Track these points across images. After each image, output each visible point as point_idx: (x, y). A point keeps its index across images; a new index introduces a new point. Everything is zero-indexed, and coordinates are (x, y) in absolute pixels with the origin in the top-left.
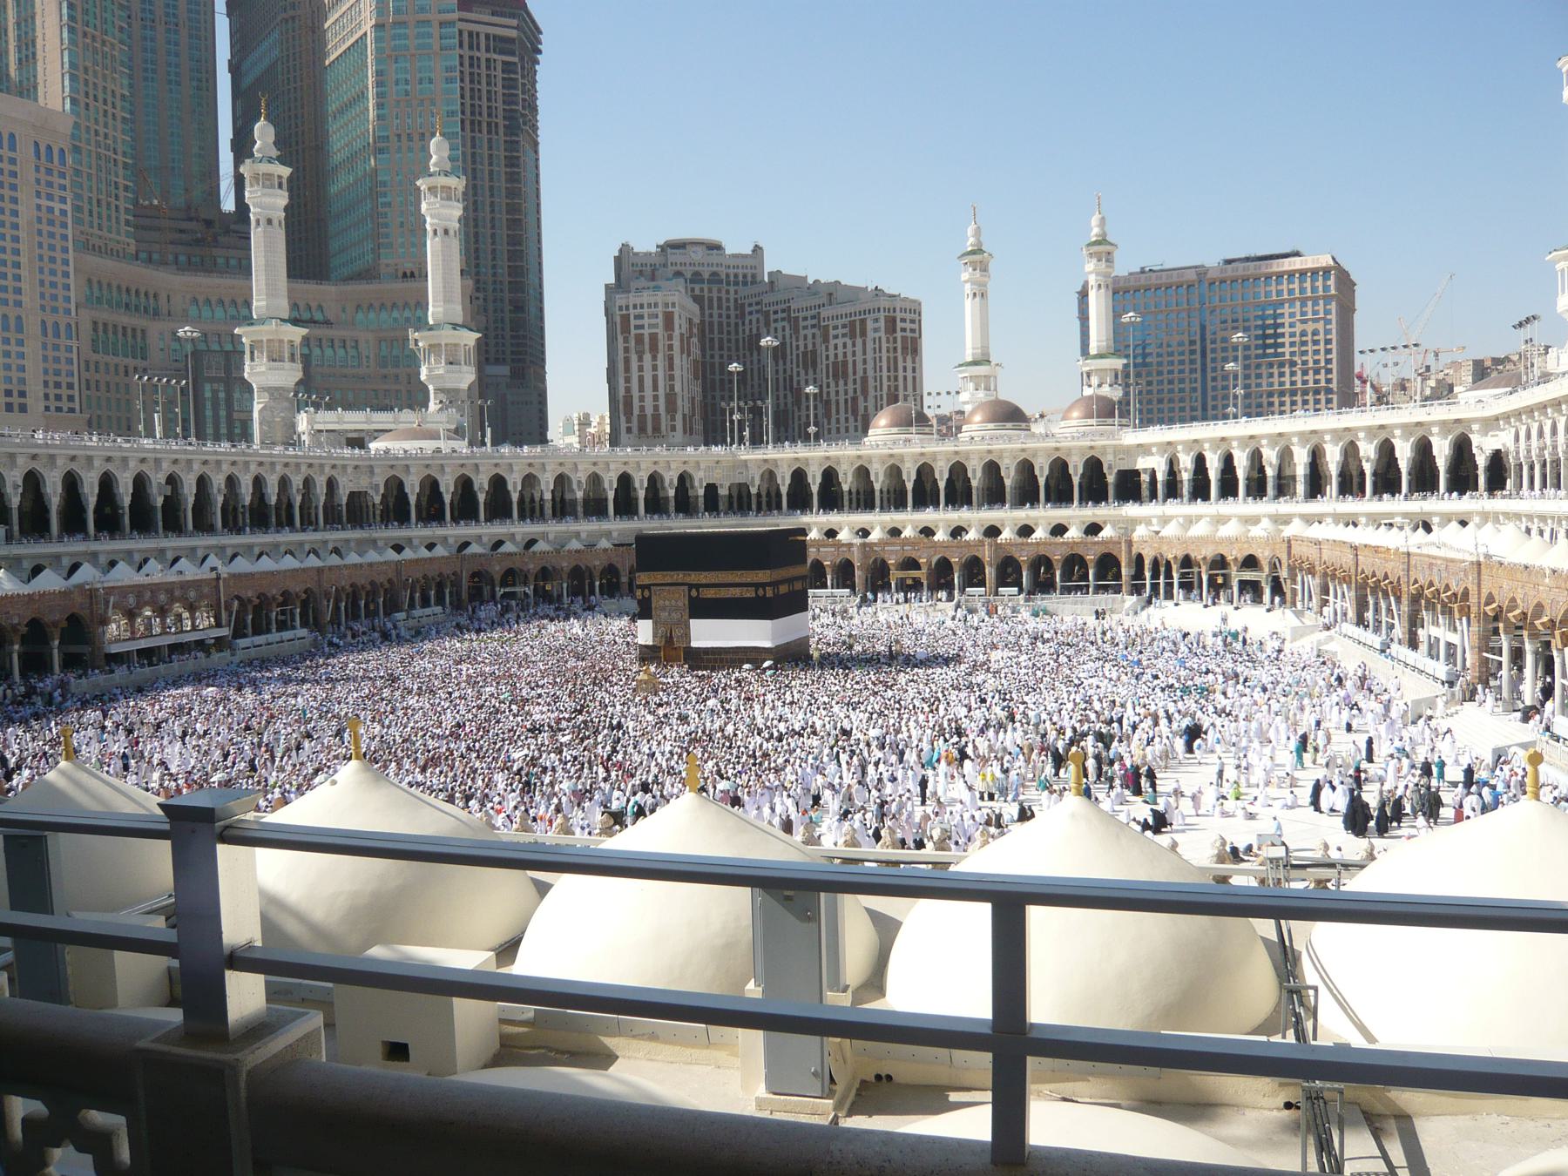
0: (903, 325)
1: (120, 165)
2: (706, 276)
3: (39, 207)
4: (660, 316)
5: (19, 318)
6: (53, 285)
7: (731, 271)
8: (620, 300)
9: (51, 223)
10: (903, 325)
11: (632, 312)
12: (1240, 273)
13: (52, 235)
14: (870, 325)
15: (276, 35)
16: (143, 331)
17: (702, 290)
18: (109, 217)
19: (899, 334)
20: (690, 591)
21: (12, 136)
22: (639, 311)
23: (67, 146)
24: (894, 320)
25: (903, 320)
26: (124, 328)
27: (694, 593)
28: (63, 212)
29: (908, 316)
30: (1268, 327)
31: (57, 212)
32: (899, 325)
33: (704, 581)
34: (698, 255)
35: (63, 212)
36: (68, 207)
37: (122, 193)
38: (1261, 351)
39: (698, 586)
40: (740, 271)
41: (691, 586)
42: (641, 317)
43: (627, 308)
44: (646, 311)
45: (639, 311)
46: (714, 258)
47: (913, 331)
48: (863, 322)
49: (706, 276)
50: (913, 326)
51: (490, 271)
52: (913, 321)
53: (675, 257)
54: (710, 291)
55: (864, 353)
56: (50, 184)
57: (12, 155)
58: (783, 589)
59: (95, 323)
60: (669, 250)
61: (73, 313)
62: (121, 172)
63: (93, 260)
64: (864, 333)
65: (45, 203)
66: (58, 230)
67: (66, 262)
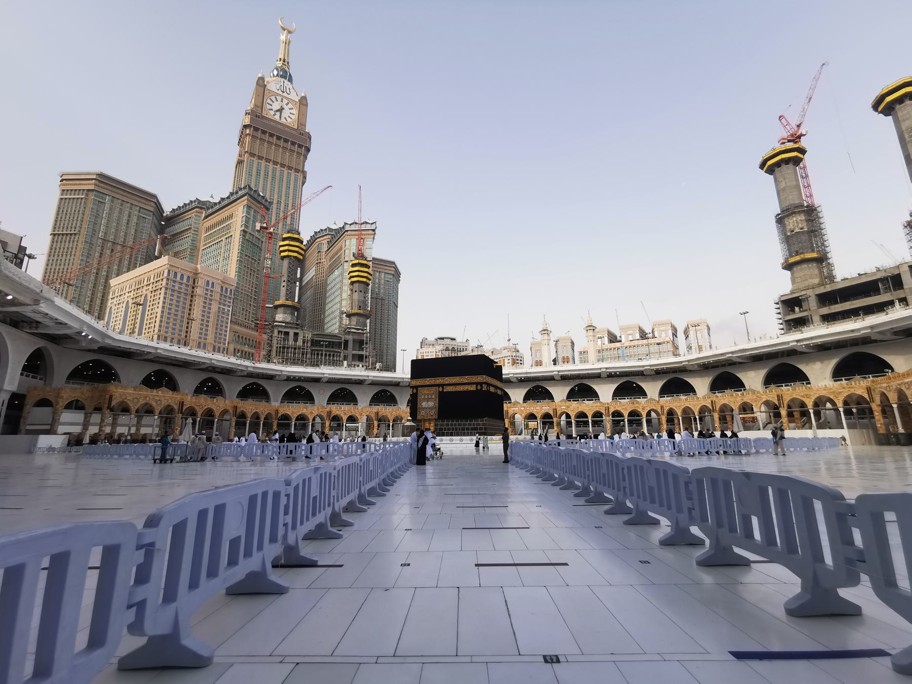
0: (517, 361)
1: (253, 298)
2: (450, 348)
3: (219, 308)
4: (434, 356)
5: (205, 344)
6: (220, 334)
7: (459, 347)
8: (421, 350)
9: (223, 313)
10: (517, 361)
11: (425, 354)
13: (223, 318)
14: (506, 361)
15: (314, 268)
16: (253, 354)
17: (449, 353)
18: (246, 314)
21: (213, 283)
22: (427, 354)
23: (233, 288)
25: (518, 360)
26: (246, 352)
27: (441, 389)
28: (229, 311)
29: (519, 359)
31: (226, 310)
34: (448, 342)
35: (229, 311)
36: (231, 309)
37: (252, 307)
39: (443, 385)
40: (462, 347)
41: (439, 385)
42: (428, 356)
43: (423, 353)
44: (430, 354)
45: (427, 354)
46: (453, 342)
48: (504, 360)
49: (450, 348)
50: (521, 362)
51: (379, 341)
52: (521, 360)
53: (440, 342)
54: (452, 353)
56: (225, 301)
57: (212, 289)
58: (492, 389)
59: (235, 349)
60: (439, 340)
61: (227, 345)
62: (252, 300)
63: (237, 328)
65: (221, 306)
66: (225, 316)
67: (227, 327)
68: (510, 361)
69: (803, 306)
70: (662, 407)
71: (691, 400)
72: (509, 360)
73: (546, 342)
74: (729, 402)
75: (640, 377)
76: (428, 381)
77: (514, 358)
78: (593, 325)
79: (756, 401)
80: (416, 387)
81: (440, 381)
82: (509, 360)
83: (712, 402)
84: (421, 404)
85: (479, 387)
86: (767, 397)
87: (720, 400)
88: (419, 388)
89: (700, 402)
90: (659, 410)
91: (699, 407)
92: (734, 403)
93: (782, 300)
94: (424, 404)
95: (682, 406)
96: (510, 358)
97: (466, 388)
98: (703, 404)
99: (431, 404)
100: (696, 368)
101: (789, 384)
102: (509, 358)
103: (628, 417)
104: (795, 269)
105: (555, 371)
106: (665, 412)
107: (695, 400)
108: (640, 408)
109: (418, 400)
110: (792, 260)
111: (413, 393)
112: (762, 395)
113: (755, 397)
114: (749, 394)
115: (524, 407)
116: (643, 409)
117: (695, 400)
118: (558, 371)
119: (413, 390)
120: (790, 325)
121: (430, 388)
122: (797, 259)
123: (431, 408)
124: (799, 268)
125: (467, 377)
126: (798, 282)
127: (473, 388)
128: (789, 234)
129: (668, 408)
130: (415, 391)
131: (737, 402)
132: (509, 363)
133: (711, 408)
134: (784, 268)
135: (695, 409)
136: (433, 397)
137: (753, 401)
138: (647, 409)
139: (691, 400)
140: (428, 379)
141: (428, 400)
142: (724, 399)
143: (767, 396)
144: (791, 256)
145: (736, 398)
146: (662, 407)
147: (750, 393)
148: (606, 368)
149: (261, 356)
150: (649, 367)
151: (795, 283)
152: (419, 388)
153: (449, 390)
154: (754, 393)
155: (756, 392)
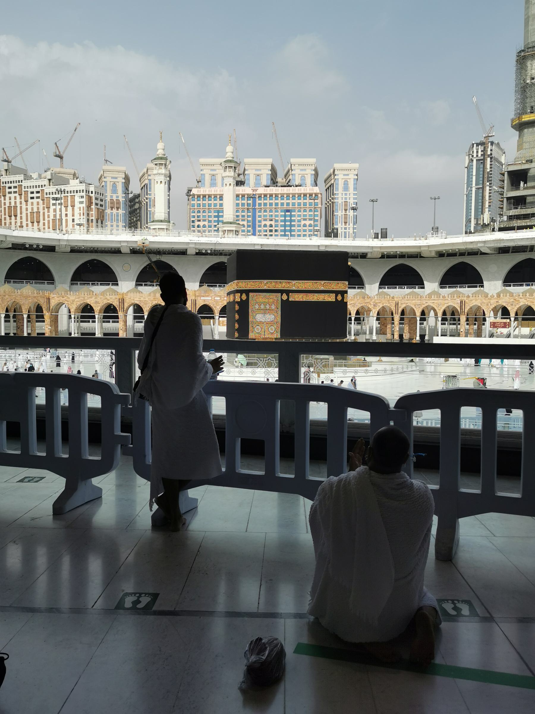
0: (97, 202)
12: (274, 192)
14: (77, 199)
19: (93, 207)
20: (282, 295)
24: (90, 198)
27: (285, 297)
30: (288, 221)
32: (94, 201)
33: (294, 288)
38: (283, 233)
39: (288, 292)
41: (281, 292)
47: (101, 206)
48: (73, 197)
50: (102, 203)
52: (102, 200)
55: (73, 215)
64: (73, 202)
68: (84, 200)
69: (528, 183)
70: (397, 304)
71: (436, 298)
72: (82, 197)
73: (162, 178)
74: (481, 304)
75: (359, 259)
76: (265, 284)
77: (91, 195)
78: (235, 160)
79: (512, 305)
80: (247, 292)
81: (283, 284)
82: (82, 197)
83: (461, 302)
84: (254, 318)
85: (339, 298)
86: (525, 301)
87: (472, 300)
88: (251, 294)
89: (446, 302)
90: (393, 308)
91: (443, 308)
92: (488, 305)
93: (509, 170)
94: (259, 317)
95: (423, 304)
96: (84, 194)
97: (321, 298)
98: (450, 304)
99: (270, 317)
100: (433, 254)
101: (531, 283)
102: (82, 194)
103: (356, 315)
104: (526, 130)
105: (258, 244)
106: (400, 310)
107: (441, 298)
108: (371, 304)
109: (250, 311)
110: (526, 118)
111: (241, 299)
112: (521, 298)
113: (513, 300)
114: (506, 296)
115: (220, 296)
116: (374, 306)
117: (441, 298)
118: (261, 245)
119: (241, 295)
120: (510, 203)
121: (268, 294)
122: (531, 118)
123: (271, 323)
124: (530, 130)
125: (323, 282)
126: (525, 149)
127: (331, 298)
128: (528, 81)
129: (403, 306)
130: (244, 297)
131: (491, 305)
132: (81, 203)
133: (459, 311)
134: (513, 127)
135: (440, 310)
136: (273, 307)
137: (509, 305)
138: (379, 306)
139: (436, 298)
140: (265, 281)
141: (265, 311)
142: (476, 300)
143: (525, 299)
144: (524, 112)
145: (491, 299)
146: (397, 304)
147: (508, 295)
148: (326, 246)
149: (18, 227)
150: (379, 250)
151: (522, 149)
152: (251, 294)
153: (297, 300)
154: (512, 296)
155: (514, 295)
